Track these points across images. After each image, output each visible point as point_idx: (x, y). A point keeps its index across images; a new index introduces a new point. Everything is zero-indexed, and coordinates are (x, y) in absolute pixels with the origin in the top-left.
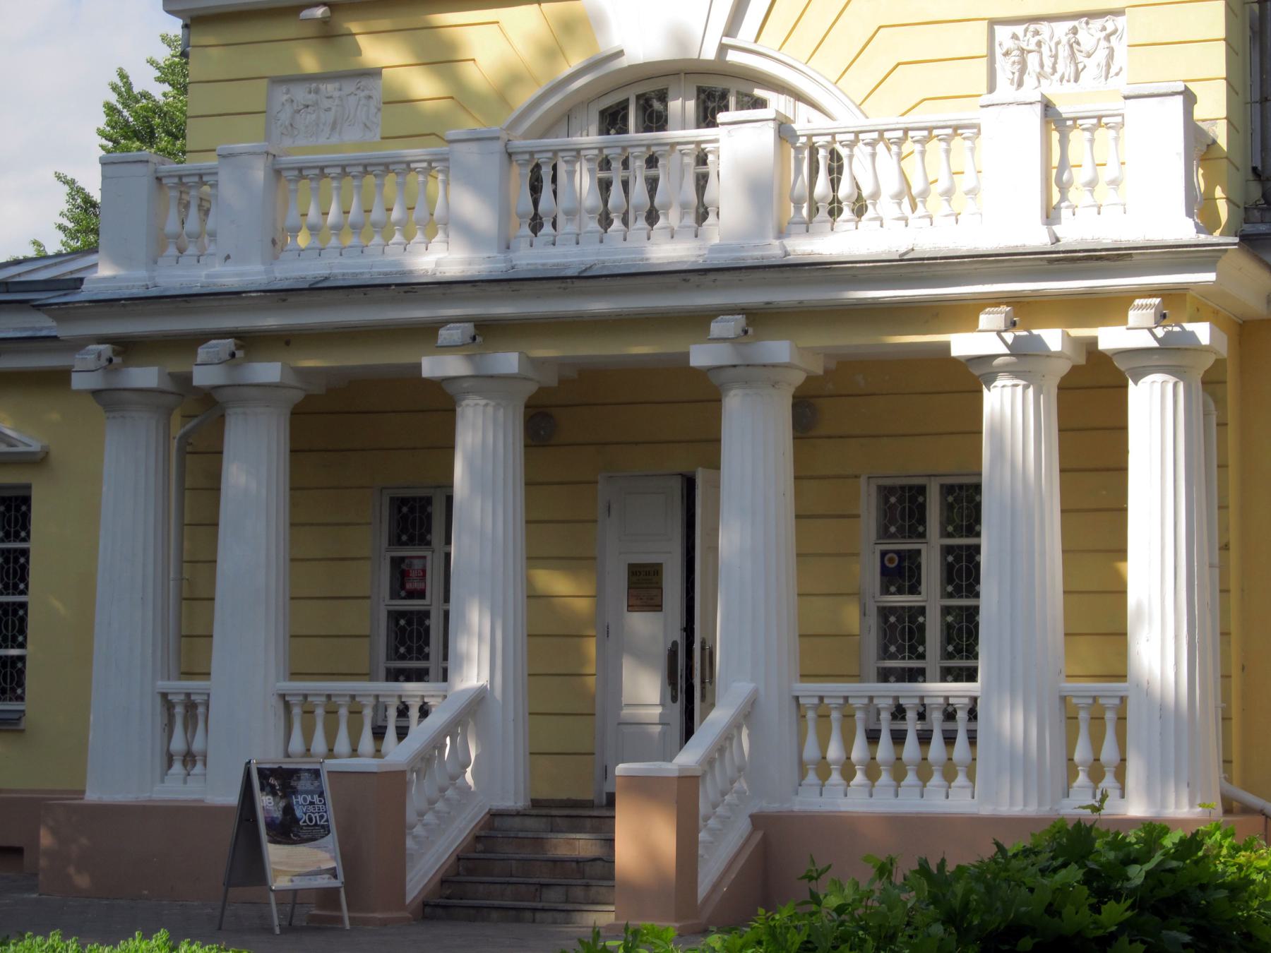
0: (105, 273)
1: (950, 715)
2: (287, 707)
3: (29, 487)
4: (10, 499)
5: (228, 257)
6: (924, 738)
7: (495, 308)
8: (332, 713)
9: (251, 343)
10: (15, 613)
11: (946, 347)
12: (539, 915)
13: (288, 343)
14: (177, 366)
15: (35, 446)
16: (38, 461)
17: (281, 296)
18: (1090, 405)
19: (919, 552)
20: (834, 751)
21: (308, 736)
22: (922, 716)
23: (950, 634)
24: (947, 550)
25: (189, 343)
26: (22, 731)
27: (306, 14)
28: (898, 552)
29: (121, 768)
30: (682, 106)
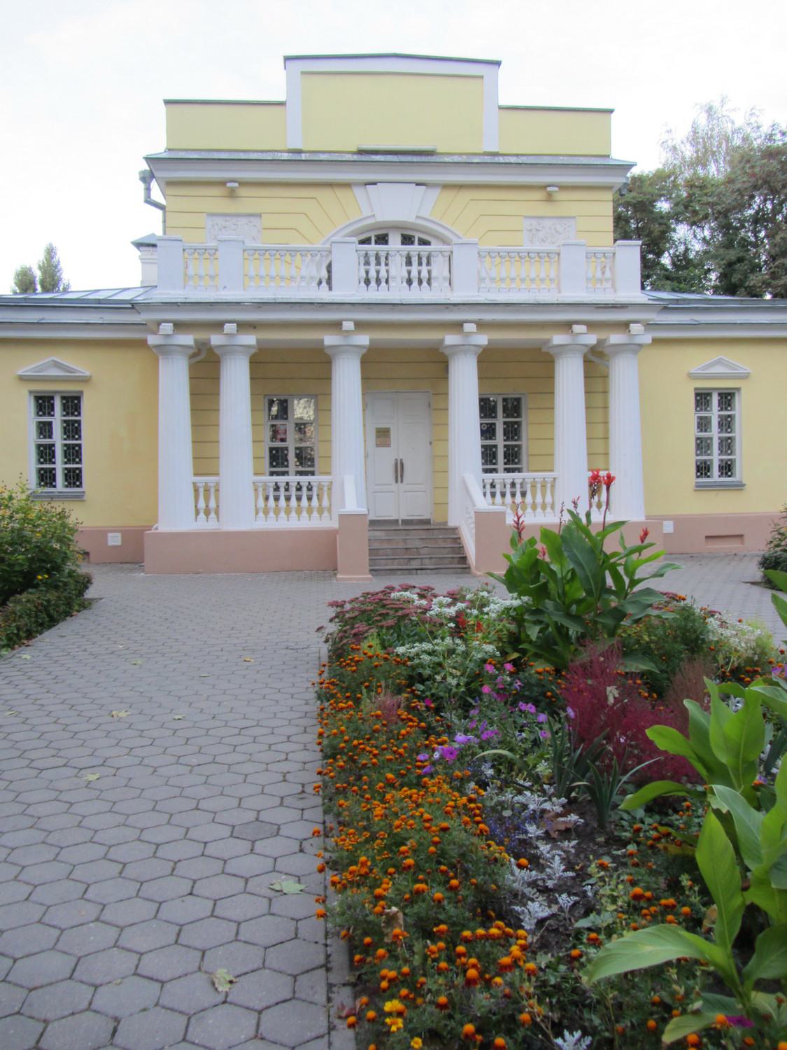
0: (158, 296)
1: (299, 489)
2: (196, 490)
3: (82, 392)
4: (68, 397)
5: (225, 287)
6: (288, 499)
7: (369, 316)
8: (544, 486)
9: (244, 326)
10: (74, 448)
11: (548, 341)
12: (419, 571)
13: (255, 328)
14: (202, 335)
15: (87, 373)
16: (86, 380)
17: (261, 305)
18: (596, 365)
19: (494, 424)
20: (539, 499)
21: (544, 496)
22: (287, 490)
23: (494, 456)
24: (505, 423)
25: (219, 326)
26: (84, 501)
27: (228, 185)
28: (487, 424)
29: (177, 515)
30: (395, 241)
